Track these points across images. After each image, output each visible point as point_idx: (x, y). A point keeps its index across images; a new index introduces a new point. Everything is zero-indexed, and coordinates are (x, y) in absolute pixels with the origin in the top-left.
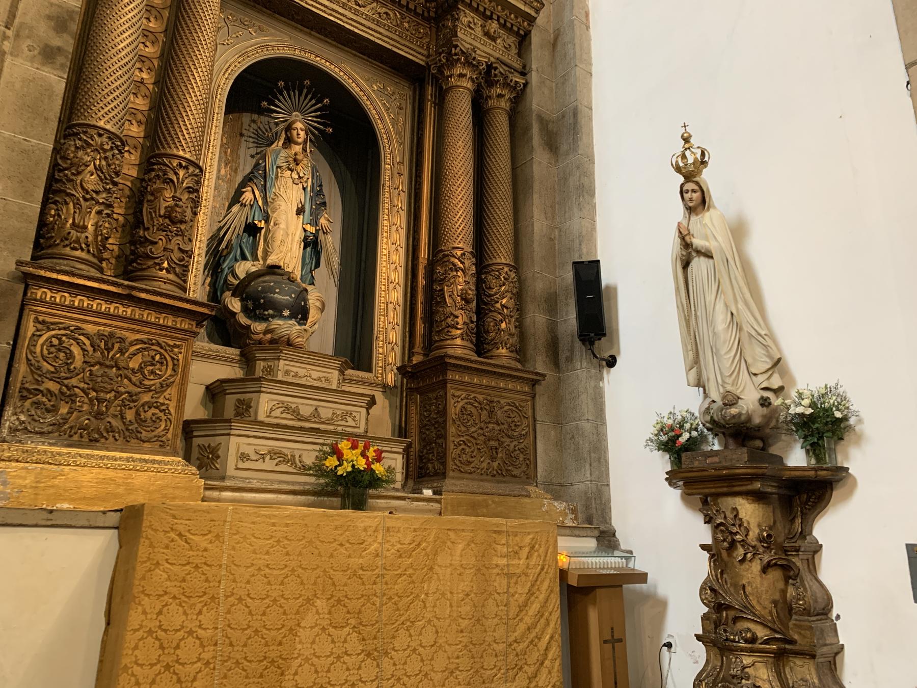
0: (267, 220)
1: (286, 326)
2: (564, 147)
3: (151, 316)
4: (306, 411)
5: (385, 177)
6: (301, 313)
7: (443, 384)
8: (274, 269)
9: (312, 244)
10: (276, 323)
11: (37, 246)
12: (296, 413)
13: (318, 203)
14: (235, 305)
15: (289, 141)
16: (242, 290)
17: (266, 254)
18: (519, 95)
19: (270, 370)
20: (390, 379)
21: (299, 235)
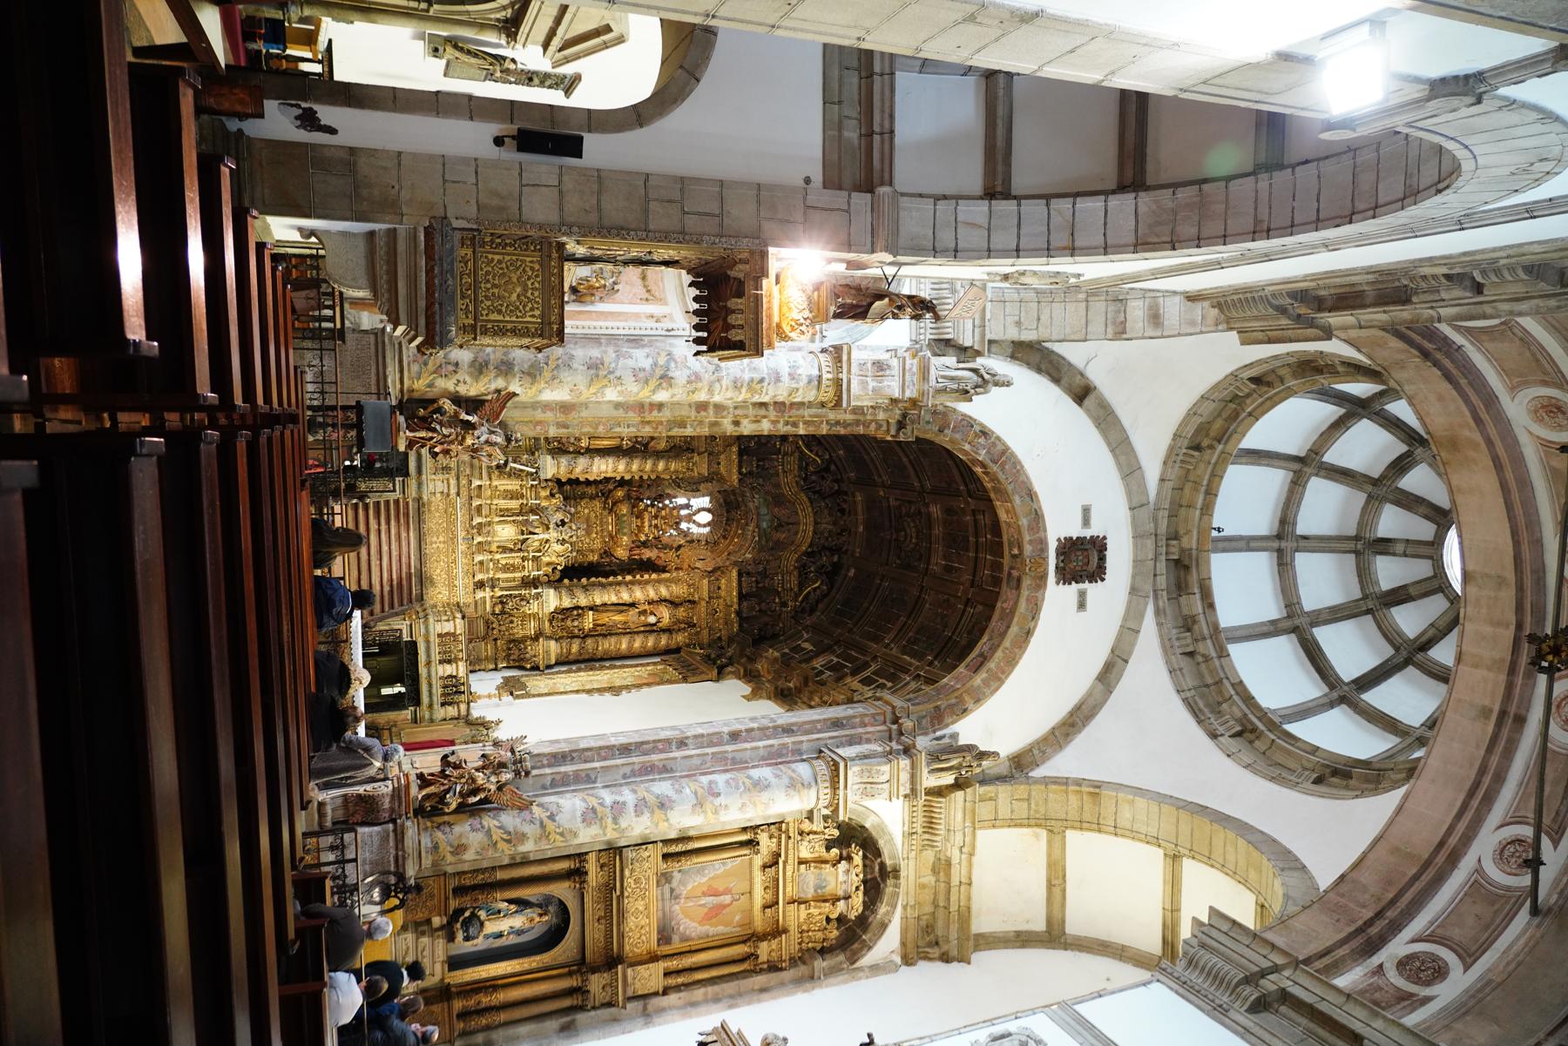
0: (504, 916)
1: (460, 936)
2: (562, 1035)
3: (443, 904)
4: (425, 953)
5: (533, 958)
6: (467, 939)
7: (442, 1001)
8: (482, 924)
9: (500, 935)
10: (461, 932)
11: (458, 873)
12: (423, 950)
13: (520, 932)
14: (467, 914)
15: (541, 915)
16: (473, 915)
17: (489, 920)
18: (581, 1008)
19: (438, 937)
20: (447, 981)
21: (502, 928)
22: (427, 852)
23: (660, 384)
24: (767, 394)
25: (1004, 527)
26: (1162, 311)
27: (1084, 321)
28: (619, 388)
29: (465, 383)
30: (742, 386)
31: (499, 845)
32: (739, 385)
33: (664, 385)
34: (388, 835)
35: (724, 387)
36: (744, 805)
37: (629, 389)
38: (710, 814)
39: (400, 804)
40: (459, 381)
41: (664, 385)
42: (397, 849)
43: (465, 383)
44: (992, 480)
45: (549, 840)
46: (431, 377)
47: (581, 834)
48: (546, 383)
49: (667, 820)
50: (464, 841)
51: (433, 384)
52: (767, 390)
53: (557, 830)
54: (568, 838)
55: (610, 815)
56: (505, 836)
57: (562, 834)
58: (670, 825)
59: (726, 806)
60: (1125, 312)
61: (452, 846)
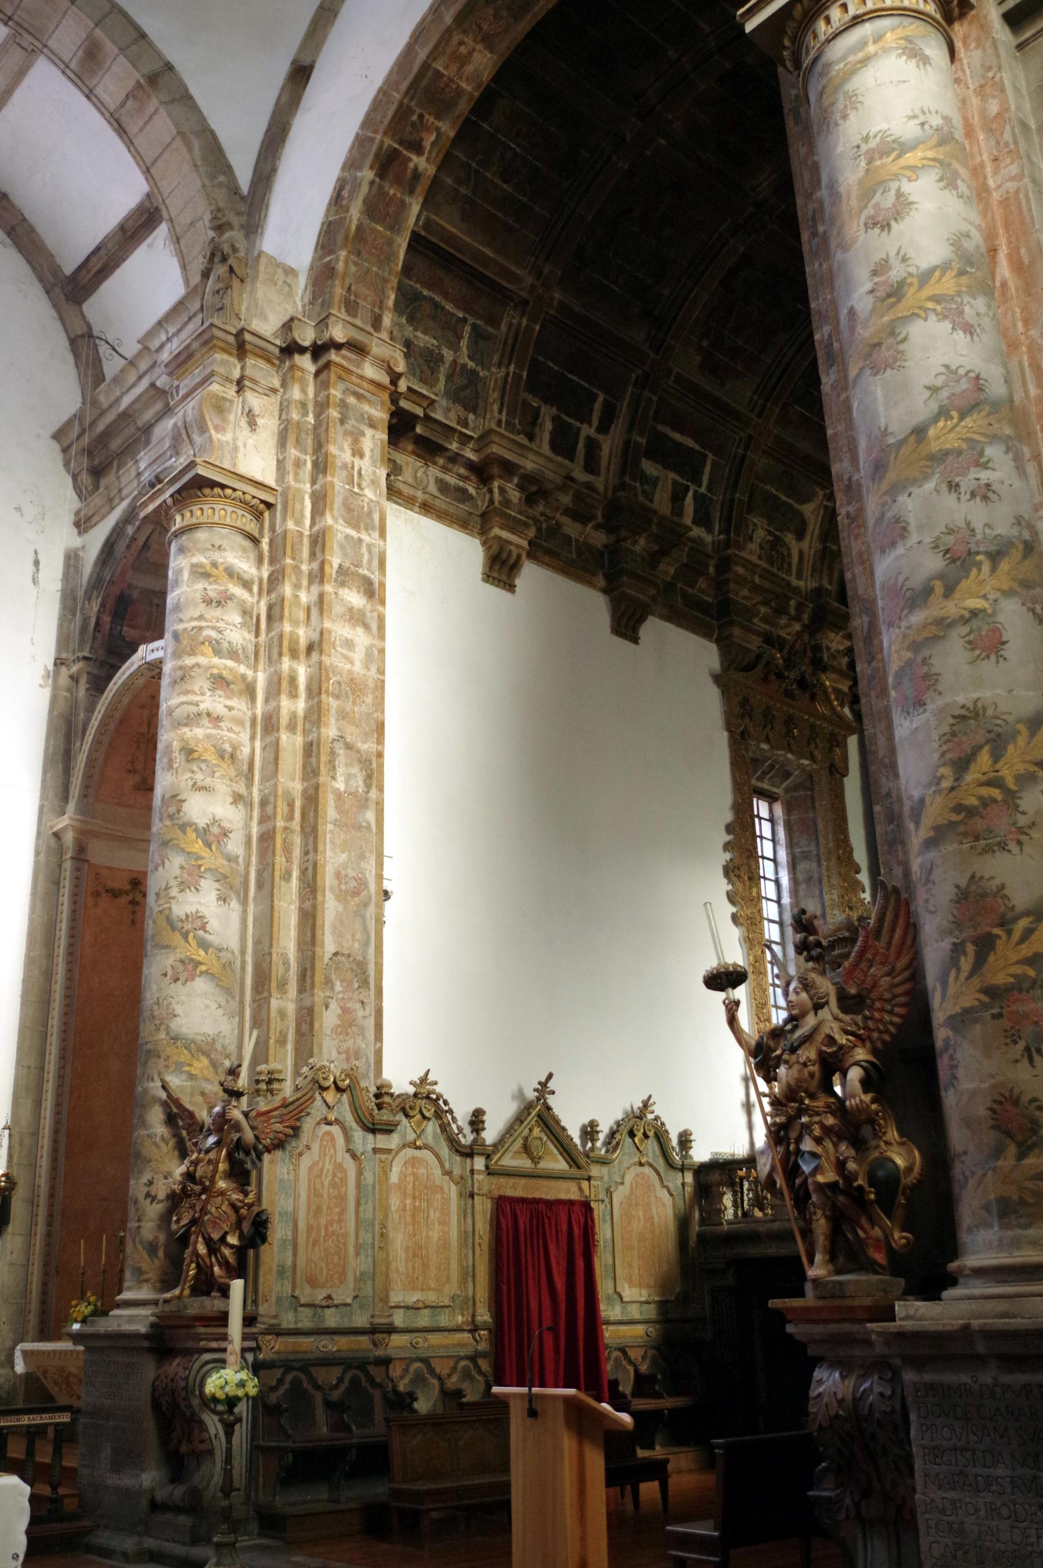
22: (1016, 1244)
23: (171, 817)
24: (201, 617)
25: (506, 44)
26: (80, 53)
27: (166, 155)
28: (174, 892)
29: (151, 1183)
30: (181, 668)
31: (1001, 979)
32: (179, 673)
33: (172, 810)
34: (931, 1387)
35: (183, 699)
36: (873, 223)
37: (177, 872)
38: (902, 309)
39: (850, 1340)
40: (148, 1195)
41: (172, 810)
42: (980, 1361)
43: (151, 1183)
44: (420, 125)
45: (986, 802)
46: (140, 1247)
47: (961, 699)
48: (158, 1030)
49: (919, 432)
50: (982, 1112)
51: (151, 1244)
52: (192, 619)
53: (946, 784)
54: (980, 737)
55: (904, 624)
56: (966, 964)
57: (962, 765)
58: (943, 413)
59: (875, 273)
60: (123, 104)
61: (998, 1152)
